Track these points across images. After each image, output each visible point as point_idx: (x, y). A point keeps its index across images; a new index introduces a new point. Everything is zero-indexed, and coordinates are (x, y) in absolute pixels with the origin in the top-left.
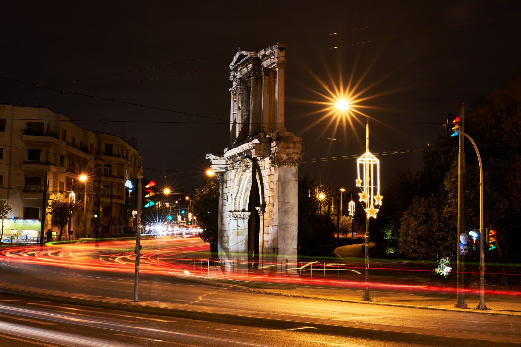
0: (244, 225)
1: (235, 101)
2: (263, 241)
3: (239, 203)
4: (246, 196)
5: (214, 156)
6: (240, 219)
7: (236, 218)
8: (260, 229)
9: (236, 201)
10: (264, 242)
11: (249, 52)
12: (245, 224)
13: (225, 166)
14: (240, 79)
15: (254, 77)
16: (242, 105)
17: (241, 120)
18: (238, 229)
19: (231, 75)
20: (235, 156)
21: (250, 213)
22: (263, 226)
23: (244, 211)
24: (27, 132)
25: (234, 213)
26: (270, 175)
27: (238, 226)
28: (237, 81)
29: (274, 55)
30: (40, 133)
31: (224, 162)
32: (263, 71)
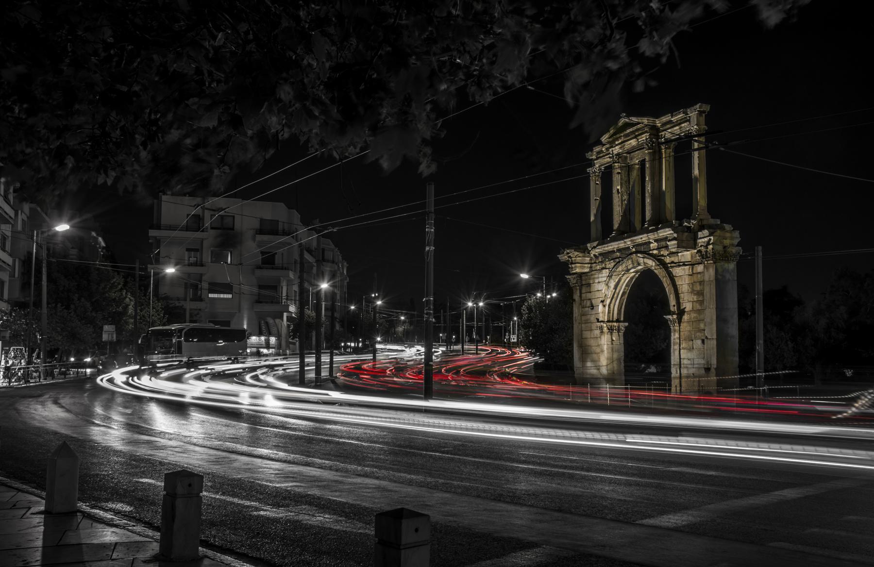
1: (597, 184)
2: (680, 359)
5: (576, 253)
6: (615, 331)
7: (611, 330)
8: (672, 344)
10: (682, 360)
11: (646, 119)
14: (618, 154)
15: (651, 151)
16: (621, 188)
20: (613, 252)
21: (627, 324)
22: (680, 340)
23: (618, 321)
24: (261, 231)
25: (608, 324)
26: (693, 273)
28: (613, 157)
29: (689, 121)
30: (274, 232)
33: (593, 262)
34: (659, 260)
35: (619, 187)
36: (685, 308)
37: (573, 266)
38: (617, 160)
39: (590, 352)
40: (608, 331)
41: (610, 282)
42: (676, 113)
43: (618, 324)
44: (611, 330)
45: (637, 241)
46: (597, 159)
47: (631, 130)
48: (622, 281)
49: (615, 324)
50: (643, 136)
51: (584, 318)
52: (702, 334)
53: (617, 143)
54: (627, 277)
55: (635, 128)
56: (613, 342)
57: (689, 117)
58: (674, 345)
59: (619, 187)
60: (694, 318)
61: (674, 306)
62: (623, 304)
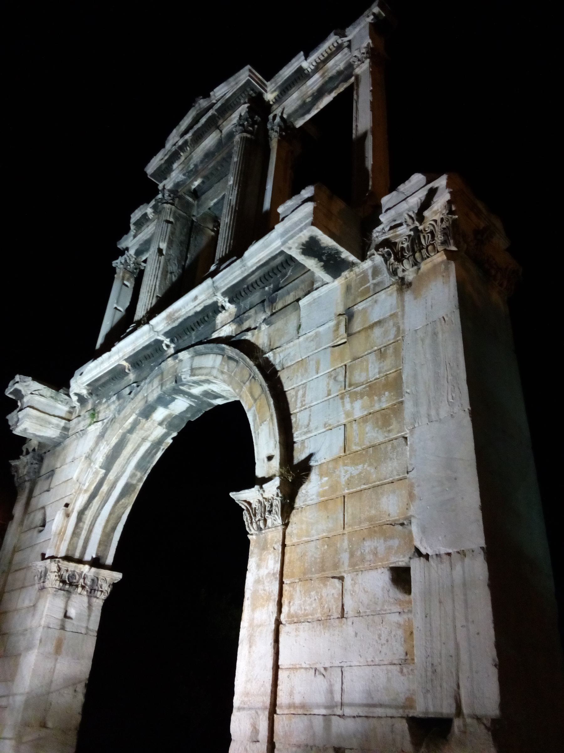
0: (89, 616)
3: (90, 531)
4: (116, 514)
6: (80, 589)
9: (81, 524)
12: (93, 614)
13: (64, 421)
16: (169, 247)
17: (159, 279)
18: (63, 628)
21: (118, 576)
22: (281, 583)
23: (97, 563)
25: (65, 565)
27: (66, 616)
31: (62, 409)
32: (279, 125)
35: (163, 246)
36: (311, 455)
38: (171, 199)
40: (58, 584)
41: (97, 449)
43: (93, 569)
44: (71, 584)
45: (183, 312)
48: (129, 448)
49: (85, 569)
52: (395, 543)
54: (144, 439)
56: (68, 622)
58: (253, 610)
59: (163, 246)
60: (349, 483)
61: (270, 458)
62: (120, 518)
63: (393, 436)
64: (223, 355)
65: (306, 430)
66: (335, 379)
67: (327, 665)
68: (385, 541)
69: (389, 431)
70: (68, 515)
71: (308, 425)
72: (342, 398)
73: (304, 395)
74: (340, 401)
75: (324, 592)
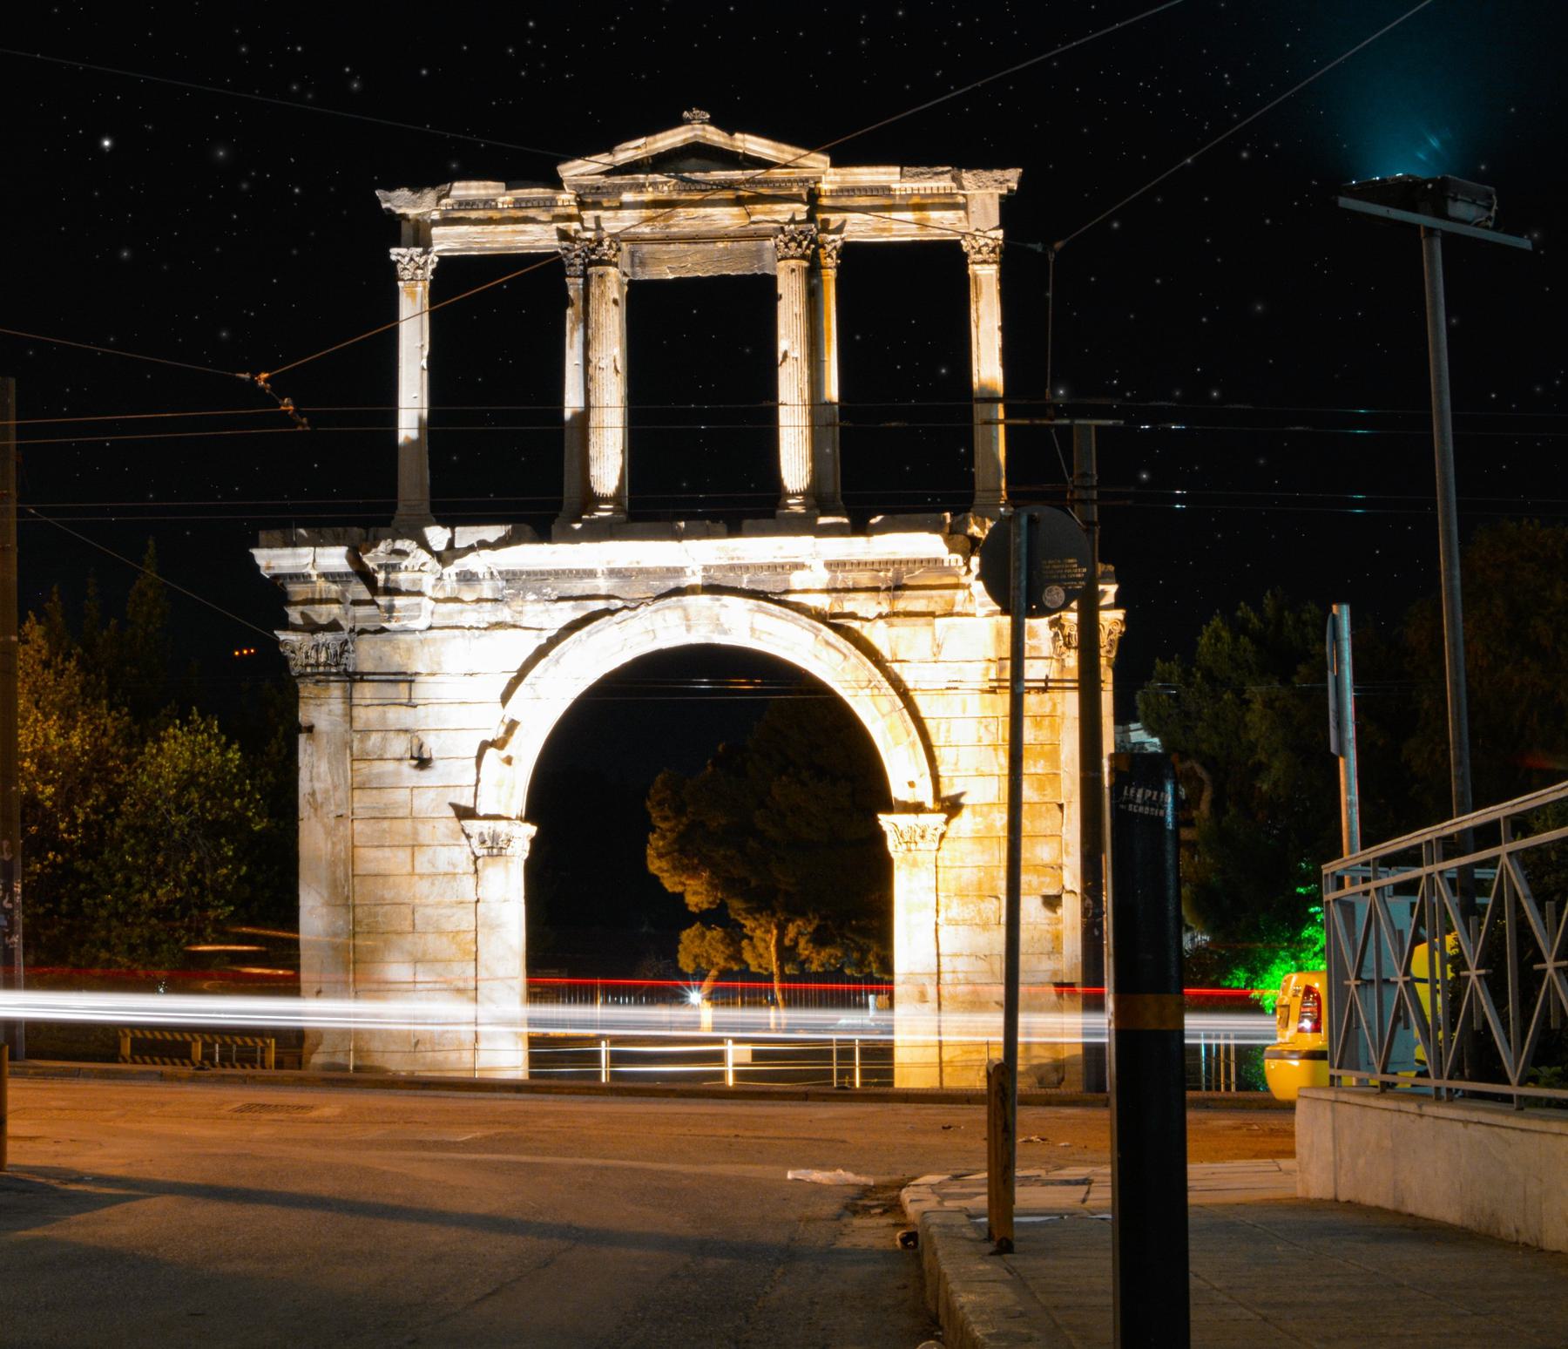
2: (938, 955)
19: (453, 193)
20: (591, 574)
28: (600, 242)
33: (441, 595)
34: (837, 628)
36: (962, 794)
37: (399, 601)
38: (615, 255)
39: (407, 926)
42: (914, 170)
46: (447, 221)
47: (737, 175)
50: (778, 207)
51: (362, 800)
52: (1048, 880)
53: (627, 197)
55: (759, 173)
57: (964, 196)
63: (1046, 799)
64: (817, 636)
65: (953, 767)
66: (986, 727)
67: (987, 953)
68: (1039, 876)
69: (1044, 795)
70: (509, 761)
71: (956, 764)
72: (995, 750)
73: (948, 731)
74: (993, 753)
75: (982, 906)
